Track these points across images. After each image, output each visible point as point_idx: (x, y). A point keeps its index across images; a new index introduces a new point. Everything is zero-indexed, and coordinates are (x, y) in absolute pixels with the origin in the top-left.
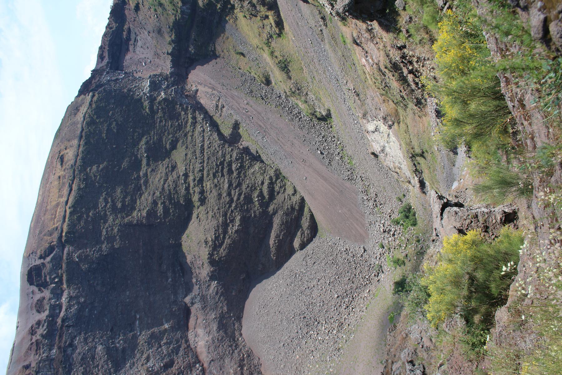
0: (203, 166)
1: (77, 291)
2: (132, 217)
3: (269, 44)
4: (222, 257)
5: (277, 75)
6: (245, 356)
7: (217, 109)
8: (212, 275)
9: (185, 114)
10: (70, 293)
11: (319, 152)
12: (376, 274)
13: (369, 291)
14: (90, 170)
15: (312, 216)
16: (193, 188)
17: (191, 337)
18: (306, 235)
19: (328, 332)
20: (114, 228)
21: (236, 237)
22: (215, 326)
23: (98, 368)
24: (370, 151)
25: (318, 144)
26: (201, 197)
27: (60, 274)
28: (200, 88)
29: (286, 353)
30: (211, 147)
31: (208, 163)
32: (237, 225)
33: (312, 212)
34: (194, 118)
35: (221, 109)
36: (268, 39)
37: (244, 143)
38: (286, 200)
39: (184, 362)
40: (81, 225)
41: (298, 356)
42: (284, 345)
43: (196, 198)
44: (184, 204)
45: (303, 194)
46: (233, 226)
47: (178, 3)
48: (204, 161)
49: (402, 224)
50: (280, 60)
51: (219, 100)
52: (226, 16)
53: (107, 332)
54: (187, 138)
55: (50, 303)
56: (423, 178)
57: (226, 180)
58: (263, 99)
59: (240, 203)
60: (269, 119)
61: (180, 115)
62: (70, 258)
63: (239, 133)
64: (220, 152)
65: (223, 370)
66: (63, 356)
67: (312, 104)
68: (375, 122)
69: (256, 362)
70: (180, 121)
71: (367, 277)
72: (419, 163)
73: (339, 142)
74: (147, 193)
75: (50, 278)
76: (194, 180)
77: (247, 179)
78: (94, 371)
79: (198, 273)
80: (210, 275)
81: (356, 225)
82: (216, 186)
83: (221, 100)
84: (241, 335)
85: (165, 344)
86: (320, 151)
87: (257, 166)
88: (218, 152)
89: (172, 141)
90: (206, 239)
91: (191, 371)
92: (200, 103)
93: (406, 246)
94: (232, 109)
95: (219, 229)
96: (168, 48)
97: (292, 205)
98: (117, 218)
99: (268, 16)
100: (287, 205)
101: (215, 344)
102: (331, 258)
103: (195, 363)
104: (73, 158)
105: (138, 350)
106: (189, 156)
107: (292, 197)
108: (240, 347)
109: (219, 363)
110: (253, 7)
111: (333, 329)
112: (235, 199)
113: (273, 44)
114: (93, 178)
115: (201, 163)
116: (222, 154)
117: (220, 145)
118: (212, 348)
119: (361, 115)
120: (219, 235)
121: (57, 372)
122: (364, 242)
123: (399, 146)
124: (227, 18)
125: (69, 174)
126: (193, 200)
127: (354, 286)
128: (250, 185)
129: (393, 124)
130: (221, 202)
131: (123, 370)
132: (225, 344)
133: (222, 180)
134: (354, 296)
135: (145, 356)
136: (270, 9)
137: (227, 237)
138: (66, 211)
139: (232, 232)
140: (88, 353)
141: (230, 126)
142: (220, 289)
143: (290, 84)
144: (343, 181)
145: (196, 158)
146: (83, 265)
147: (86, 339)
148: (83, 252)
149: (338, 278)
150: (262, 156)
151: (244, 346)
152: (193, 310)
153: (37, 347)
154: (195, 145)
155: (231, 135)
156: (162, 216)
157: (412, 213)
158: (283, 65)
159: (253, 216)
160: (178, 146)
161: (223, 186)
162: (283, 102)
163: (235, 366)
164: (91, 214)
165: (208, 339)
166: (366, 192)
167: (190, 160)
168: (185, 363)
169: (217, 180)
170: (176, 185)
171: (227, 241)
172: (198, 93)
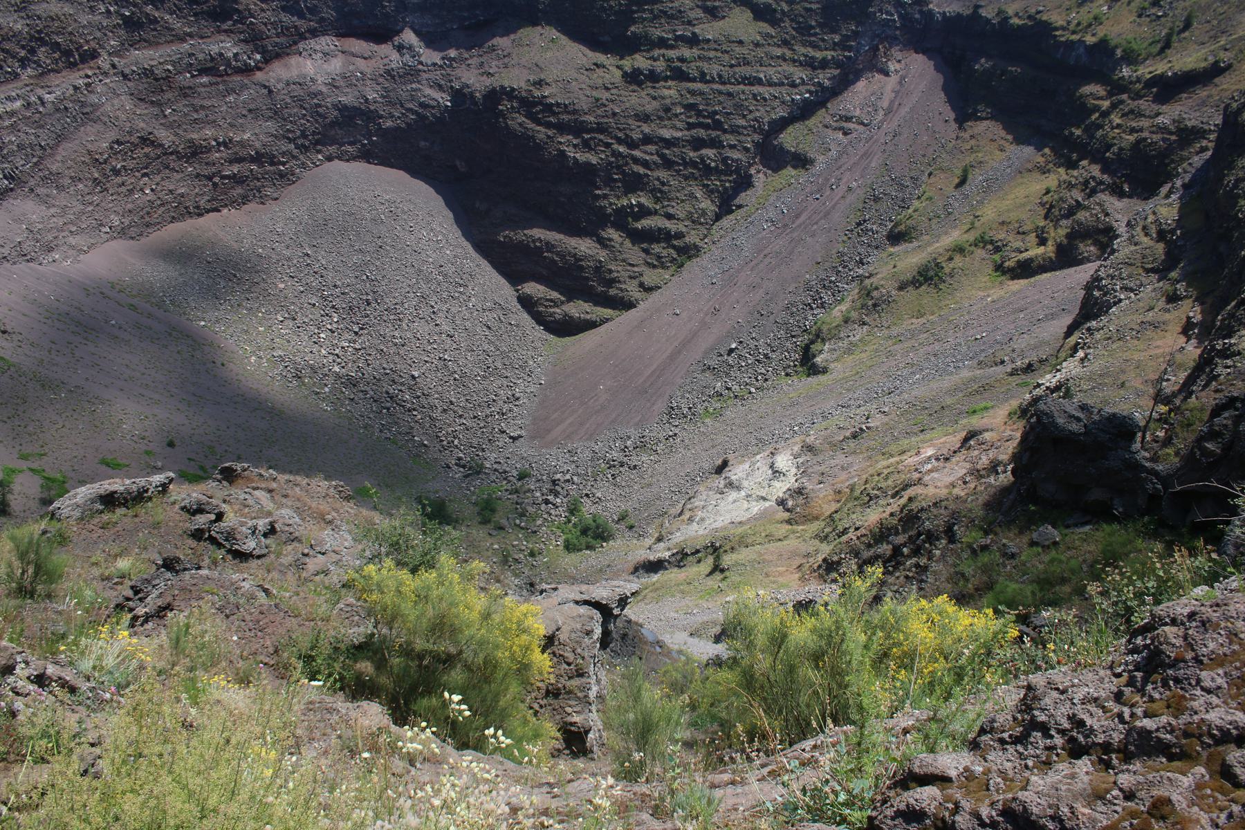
0: (713, 81)
3: (981, 245)
4: (505, 119)
5: (909, 258)
6: (282, 168)
7: (841, 118)
8: (464, 95)
9: (835, 44)
11: (733, 346)
12: (463, 462)
13: (425, 445)
15: (591, 325)
16: (663, 56)
17: (324, 44)
18: (552, 310)
19: (337, 355)
21: (550, 153)
22: (348, 98)
24: (730, 457)
25: (752, 343)
26: (642, 73)
28: (892, 81)
29: (289, 259)
30: (755, 102)
31: (720, 93)
32: (577, 156)
33: (600, 325)
34: (824, 64)
35: (841, 129)
36: (992, 242)
37: (761, 178)
38: (629, 268)
39: (265, 24)
41: (282, 286)
42: (308, 255)
43: (640, 61)
44: (629, 33)
45: (642, 306)
46: (575, 146)
47: (1093, 35)
48: (724, 83)
49: (569, 521)
50: (942, 268)
51: (862, 124)
52: (1052, 149)
54: (779, 46)
56: (667, 569)
57: (679, 134)
58: (859, 224)
59: (627, 164)
60: (813, 236)
61: (833, 31)
63: (785, 167)
64: (742, 122)
65: (250, 117)
67: (842, 335)
68: (794, 470)
69: (269, 191)
70: (818, 30)
71: (456, 442)
72: (699, 561)
73: (753, 390)
76: (682, 60)
77: (680, 182)
79: (469, 62)
80: (466, 90)
81: (568, 421)
82: (667, 110)
83: (861, 128)
86: (736, 348)
87: (708, 206)
88: (744, 116)
89: (775, 11)
90: (547, 84)
91: (245, 41)
92: (857, 79)
93: (522, 528)
94: (840, 154)
95: (569, 113)
96: (990, 8)
97: (619, 282)
99: (1044, 245)
100: (618, 270)
101: (306, 96)
102: (499, 365)
103: (263, 52)
106: (738, 49)
107: (636, 282)
108: (301, 157)
109: (264, 107)
110: (1069, 211)
111: (343, 364)
112: (636, 153)
113: (980, 253)
115: (720, 76)
116: (738, 126)
117: (758, 122)
118: (298, 91)
119: (810, 440)
120: (554, 114)
122: (533, 438)
123: (739, 519)
124: (1047, 150)
126: (637, 56)
127: (436, 414)
128: (665, 188)
129: (788, 510)
130: (630, 121)
132: (308, 121)
133: (679, 125)
134: (415, 413)
136: (1060, 248)
137: (550, 133)
139: (561, 143)
141: (801, 146)
143: (889, 287)
144: (667, 396)
145: (732, 66)
149: (455, 379)
150: (731, 217)
151: (304, 166)
152: (386, 49)
154: (761, 65)
155: (782, 148)
157: (593, 542)
158: (931, 273)
159: (598, 192)
160: (761, 24)
161: (665, 126)
162: (850, 270)
163: (258, 145)
165: (319, 82)
166: (642, 446)
167: (727, 52)
169: (681, 114)
170: (672, 17)
171: (541, 132)
172: (881, 77)
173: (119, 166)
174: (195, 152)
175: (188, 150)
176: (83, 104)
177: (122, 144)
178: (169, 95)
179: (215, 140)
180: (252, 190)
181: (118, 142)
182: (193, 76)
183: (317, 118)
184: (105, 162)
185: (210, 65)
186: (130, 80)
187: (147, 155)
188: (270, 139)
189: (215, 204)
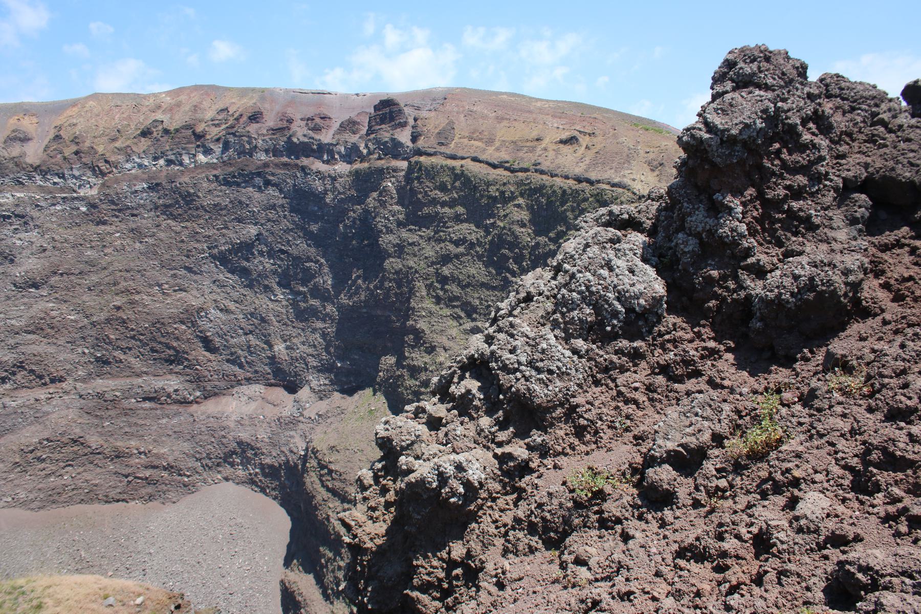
1: (342, 190)
2: (422, 297)
10: (341, 177)
14: (519, 206)
20: (416, 259)
22: (244, 436)
23: (222, 228)
27: (371, 157)
39: (209, 371)
40: (431, 191)
53: (280, 243)
55: (337, 144)
62: (389, 173)
65: (175, 436)
66: (251, 173)
69: (171, 495)
74: (454, 332)
75: (370, 140)
78: (219, 222)
84: (227, 479)
85: (248, 342)
90: (337, 450)
98: (429, 266)
101: (216, 430)
104: (552, 167)
105: (245, 295)
109: (187, 431)
114: (502, 213)
118: (212, 423)
121: (230, 164)
125: (527, 159)
131: (215, 270)
135: (232, 306)
138: (463, 158)
139: (330, 508)
140: (249, 212)
142: (293, 459)
146: (374, 199)
147: (273, 207)
148: (392, 198)
151: (205, 481)
153: (276, 130)
156: (411, 362)
163: (171, 459)
164: (446, 210)
165: (232, 419)
168: (208, 373)
171: (321, 494)
173: (44, 456)
174: (118, 455)
175: (113, 453)
176: (38, 411)
177: (52, 441)
178: (110, 413)
179: (137, 449)
180: (159, 491)
181: (47, 440)
182: (138, 401)
183: (221, 445)
184: (32, 452)
185: (155, 395)
186: (84, 399)
187: (75, 453)
188: (181, 456)
189: (125, 496)
